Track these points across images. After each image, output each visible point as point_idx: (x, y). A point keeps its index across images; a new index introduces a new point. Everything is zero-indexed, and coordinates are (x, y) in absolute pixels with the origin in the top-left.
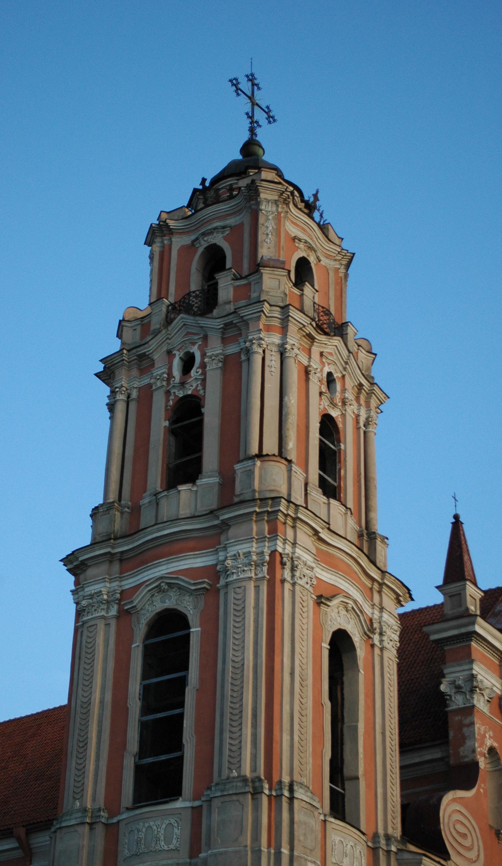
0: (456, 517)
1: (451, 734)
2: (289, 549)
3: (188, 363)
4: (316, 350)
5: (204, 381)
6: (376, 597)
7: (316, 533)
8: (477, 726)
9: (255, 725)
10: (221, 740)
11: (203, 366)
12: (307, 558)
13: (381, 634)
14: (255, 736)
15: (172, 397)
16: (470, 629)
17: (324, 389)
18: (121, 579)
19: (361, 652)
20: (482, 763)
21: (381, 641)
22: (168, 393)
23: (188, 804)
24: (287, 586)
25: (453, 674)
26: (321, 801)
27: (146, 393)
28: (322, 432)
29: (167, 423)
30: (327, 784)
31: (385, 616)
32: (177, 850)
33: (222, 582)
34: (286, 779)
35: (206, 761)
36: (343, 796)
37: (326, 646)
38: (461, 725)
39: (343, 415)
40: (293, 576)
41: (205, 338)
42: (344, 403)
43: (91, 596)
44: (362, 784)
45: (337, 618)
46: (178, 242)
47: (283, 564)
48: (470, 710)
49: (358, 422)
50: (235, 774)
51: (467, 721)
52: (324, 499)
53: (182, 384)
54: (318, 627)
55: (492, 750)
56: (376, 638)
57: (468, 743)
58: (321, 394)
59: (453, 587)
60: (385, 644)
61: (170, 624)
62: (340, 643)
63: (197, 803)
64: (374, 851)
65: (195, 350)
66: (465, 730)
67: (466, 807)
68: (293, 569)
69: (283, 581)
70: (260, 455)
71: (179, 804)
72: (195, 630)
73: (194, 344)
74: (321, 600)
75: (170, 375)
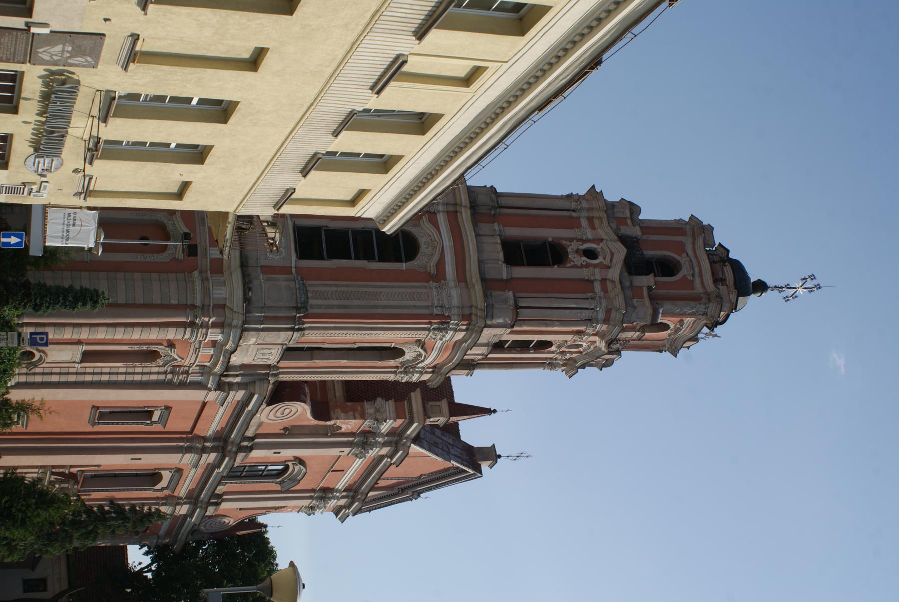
0: (495, 411)
1: (349, 404)
3: (591, 254)
9: (339, 307)
10: (331, 286)
11: (587, 266)
14: (332, 307)
15: (568, 243)
16: (416, 419)
19: (391, 363)
22: (571, 240)
23: (293, 265)
25: (389, 406)
29: (550, 239)
32: (266, 258)
35: (320, 275)
38: (354, 410)
39: (553, 352)
40: (434, 329)
47: (442, 323)
48: (363, 417)
50: (310, 295)
51: (357, 414)
55: (340, 428)
57: (343, 415)
62: (397, 352)
63: (294, 270)
64: (269, 367)
66: (351, 413)
67: (300, 415)
68: (439, 329)
69: (430, 323)
71: (294, 258)
72: (404, 266)
73: (604, 258)
74: (421, 343)
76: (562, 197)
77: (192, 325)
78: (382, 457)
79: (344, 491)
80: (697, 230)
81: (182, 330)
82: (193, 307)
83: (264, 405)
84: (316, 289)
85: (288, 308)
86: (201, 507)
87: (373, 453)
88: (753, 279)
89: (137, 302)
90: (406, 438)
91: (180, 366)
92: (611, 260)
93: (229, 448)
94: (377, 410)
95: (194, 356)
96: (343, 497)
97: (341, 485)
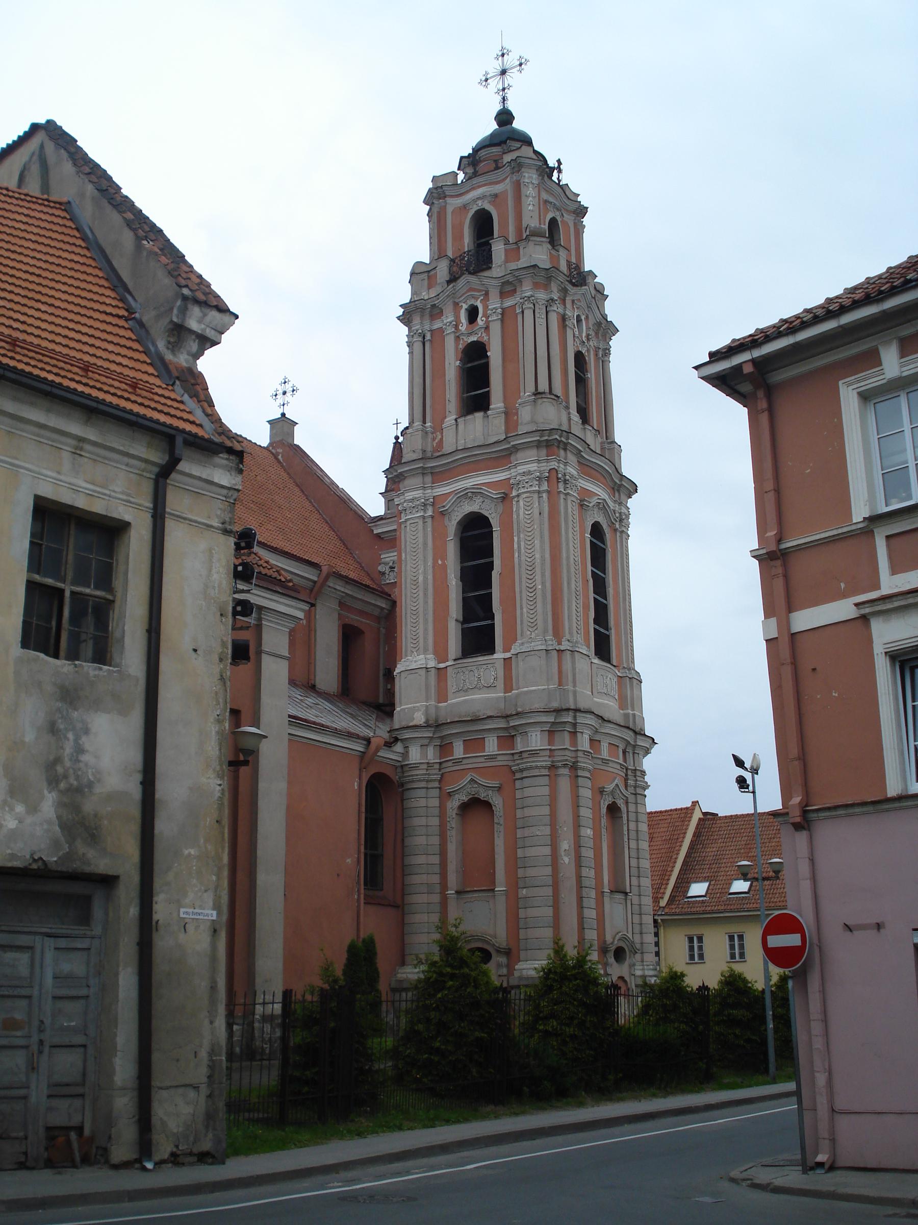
3: (473, 314)
5: (487, 328)
6: (617, 494)
18: (432, 488)
22: (457, 338)
24: (562, 496)
26: (588, 647)
27: (438, 334)
33: (514, 493)
41: (487, 294)
43: (412, 500)
46: (454, 203)
65: (479, 304)
72: (496, 528)
76: (411, 353)
80: (439, 195)
88: (495, 126)
91: (626, 780)
92: (479, 291)
95: (611, 764)
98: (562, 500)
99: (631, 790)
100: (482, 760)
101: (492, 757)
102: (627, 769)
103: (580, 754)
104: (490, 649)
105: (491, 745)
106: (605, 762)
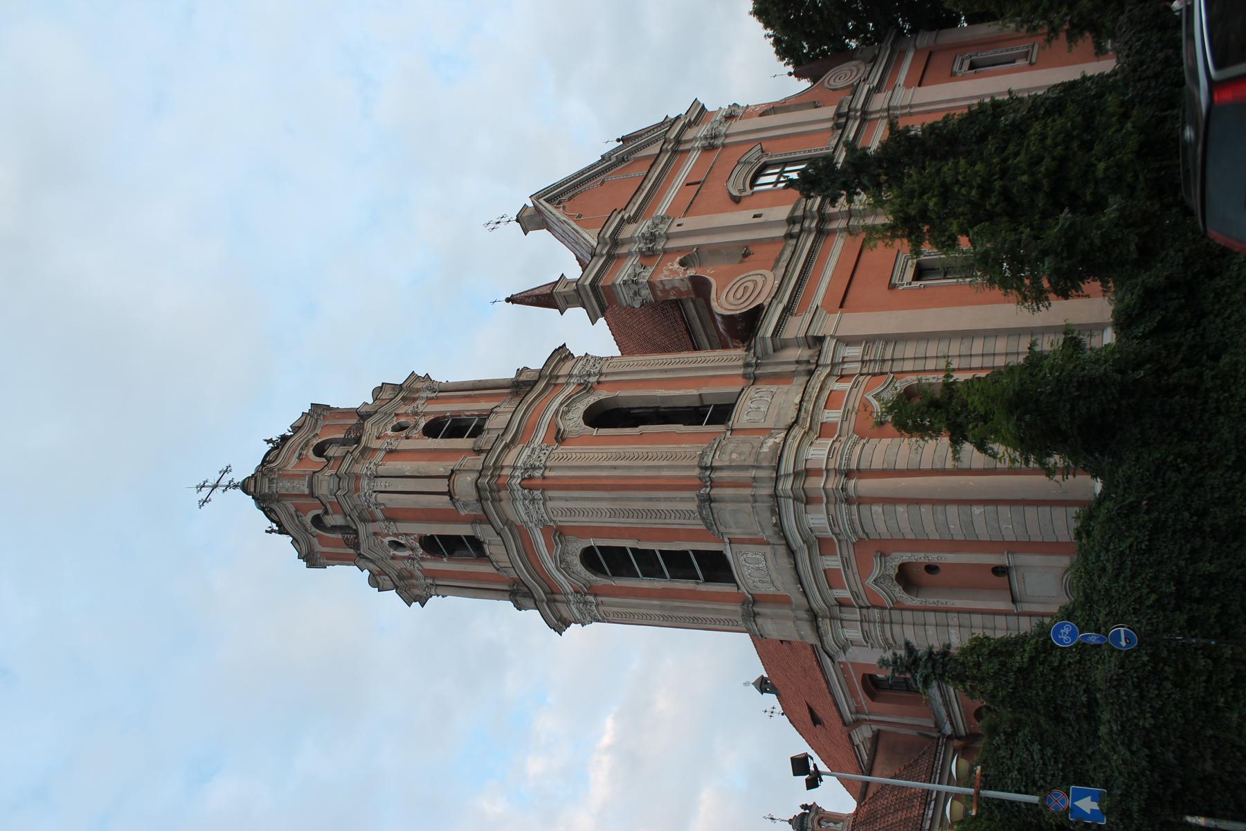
0: (508, 300)
2: (518, 473)
3: (396, 545)
4: (375, 444)
6: (561, 381)
7: (507, 446)
8: (663, 278)
11: (396, 535)
12: (527, 452)
13: (589, 375)
14: (666, 499)
16: (588, 288)
17: (403, 434)
19: (602, 394)
20: (691, 272)
21: (595, 374)
22: (422, 559)
24: (547, 473)
28: (436, 437)
30: (704, 428)
31: (575, 372)
34: (696, 472)
35: (691, 535)
36: (716, 406)
37: (595, 431)
38: (664, 291)
39: (425, 414)
40: (539, 468)
41: (375, 534)
42: (416, 414)
44: (704, 391)
45: (574, 421)
47: (530, 477)
49: (432, 398)
51: (661, 286)
52: (485, 433)
53: (412, 549)
54: (582, 440)
55: (682, 263)
56: (593, 379)
57: (677, 284)
58: (407, 438)
59: (560, 301)
60: (596, 371)
61: (590, 558)
67: (725, 286)
68: (534, 468)
69: (544, 478)
70: (449, 493)
72: (592, 542)
74: (560, 437)
75: (409, 558)
77: (848, 474)
78: (633, 219)
79: (689, 151)
81: (862, 467)
82: (848, 501)
83: (766, 304)
84: (691, 521)
85: (721, 500)
86: (856, 111)
87: (643, 227)
89: (929, 507)
90: (602, 256)
93: (813, 225)
94: (636, 293)
96: (691, 141)
97: (694, 157)
98: (552, 474)
99: (887, 368)
100: (850, 573)
101: (846, 563)
102: (861, 375)
103: (831, 466)
104: (720, 556)
105: (833, 562)
106: (845, 417)
